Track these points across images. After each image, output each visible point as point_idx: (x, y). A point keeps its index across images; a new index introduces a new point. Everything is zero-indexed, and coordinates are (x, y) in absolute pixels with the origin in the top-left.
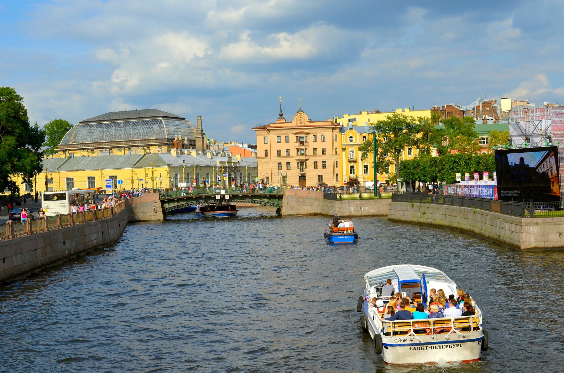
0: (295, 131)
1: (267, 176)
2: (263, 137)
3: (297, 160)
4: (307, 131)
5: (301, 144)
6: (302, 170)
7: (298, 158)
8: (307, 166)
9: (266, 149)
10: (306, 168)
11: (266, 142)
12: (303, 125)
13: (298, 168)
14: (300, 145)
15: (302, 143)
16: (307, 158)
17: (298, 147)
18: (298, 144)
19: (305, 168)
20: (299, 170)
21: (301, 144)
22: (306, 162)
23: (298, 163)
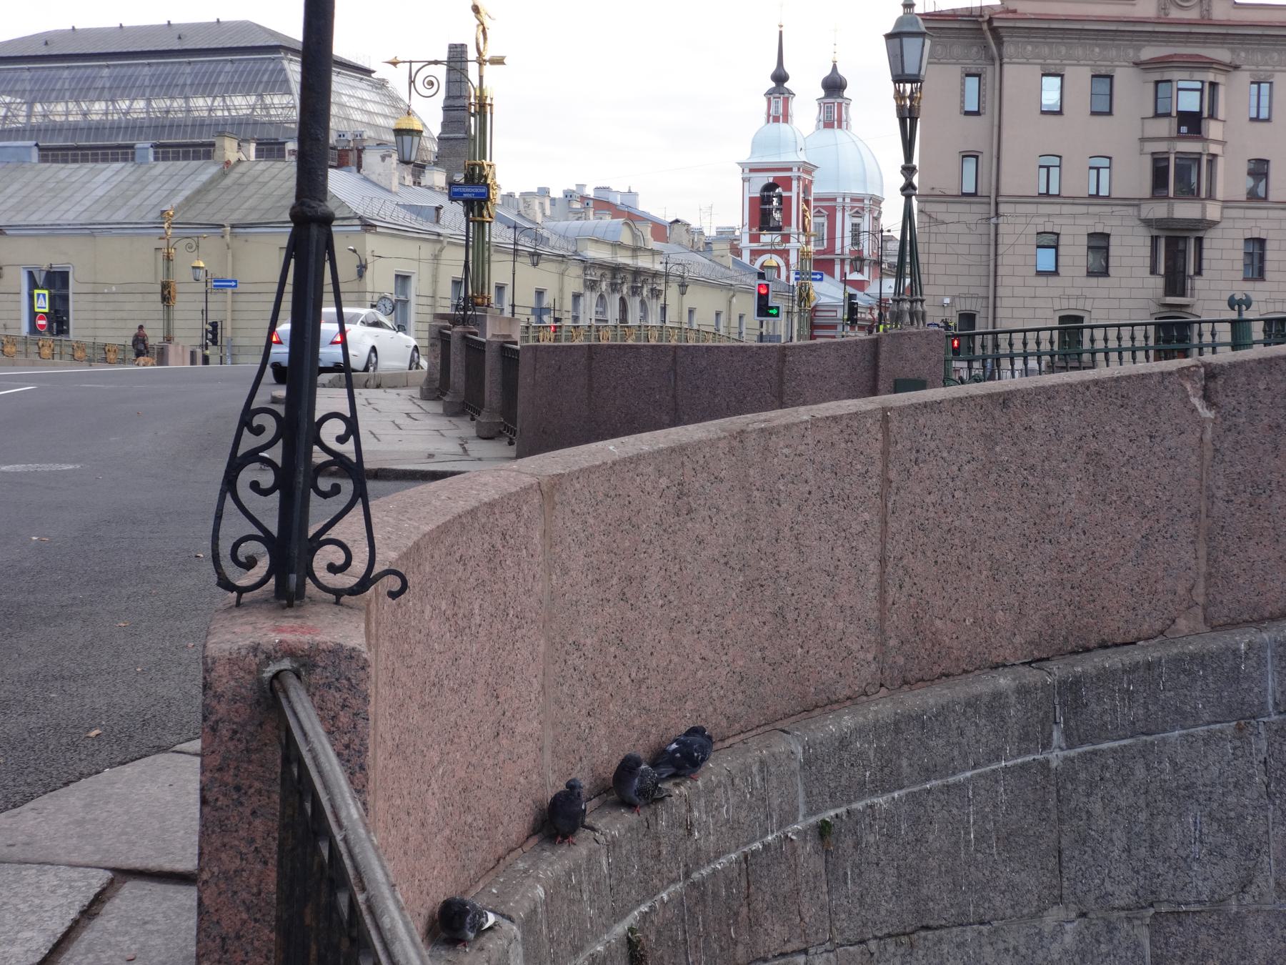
0: (1148, 53)
1: (967, 306)
2: (956, 71)
3: (1148, 223)
4: (1222, 54)
5: (1184, 129)
6: (1176, 282)
7: (1159, 210)
8: (1205, 264)
9: (970, 147)
10: (1199, 272)
11: (972, 105)
12: (1193, 15)
13: (1153, 271)
14: (1180, 137)
15: (1192, 123)
16: (1213, 211)
17: (1161, 147)
18: (1165, 127)
19: (1191, 270)
20: (1159, 282)
21: (1184, 129)
22: (1199, 241)
23: (1155, 240)
